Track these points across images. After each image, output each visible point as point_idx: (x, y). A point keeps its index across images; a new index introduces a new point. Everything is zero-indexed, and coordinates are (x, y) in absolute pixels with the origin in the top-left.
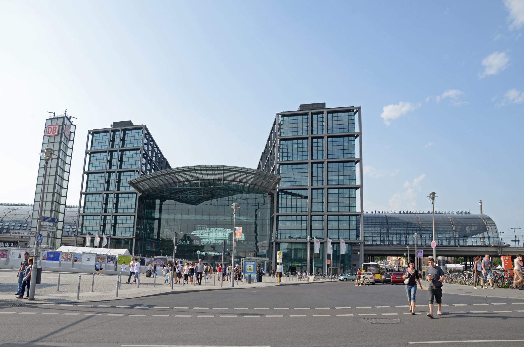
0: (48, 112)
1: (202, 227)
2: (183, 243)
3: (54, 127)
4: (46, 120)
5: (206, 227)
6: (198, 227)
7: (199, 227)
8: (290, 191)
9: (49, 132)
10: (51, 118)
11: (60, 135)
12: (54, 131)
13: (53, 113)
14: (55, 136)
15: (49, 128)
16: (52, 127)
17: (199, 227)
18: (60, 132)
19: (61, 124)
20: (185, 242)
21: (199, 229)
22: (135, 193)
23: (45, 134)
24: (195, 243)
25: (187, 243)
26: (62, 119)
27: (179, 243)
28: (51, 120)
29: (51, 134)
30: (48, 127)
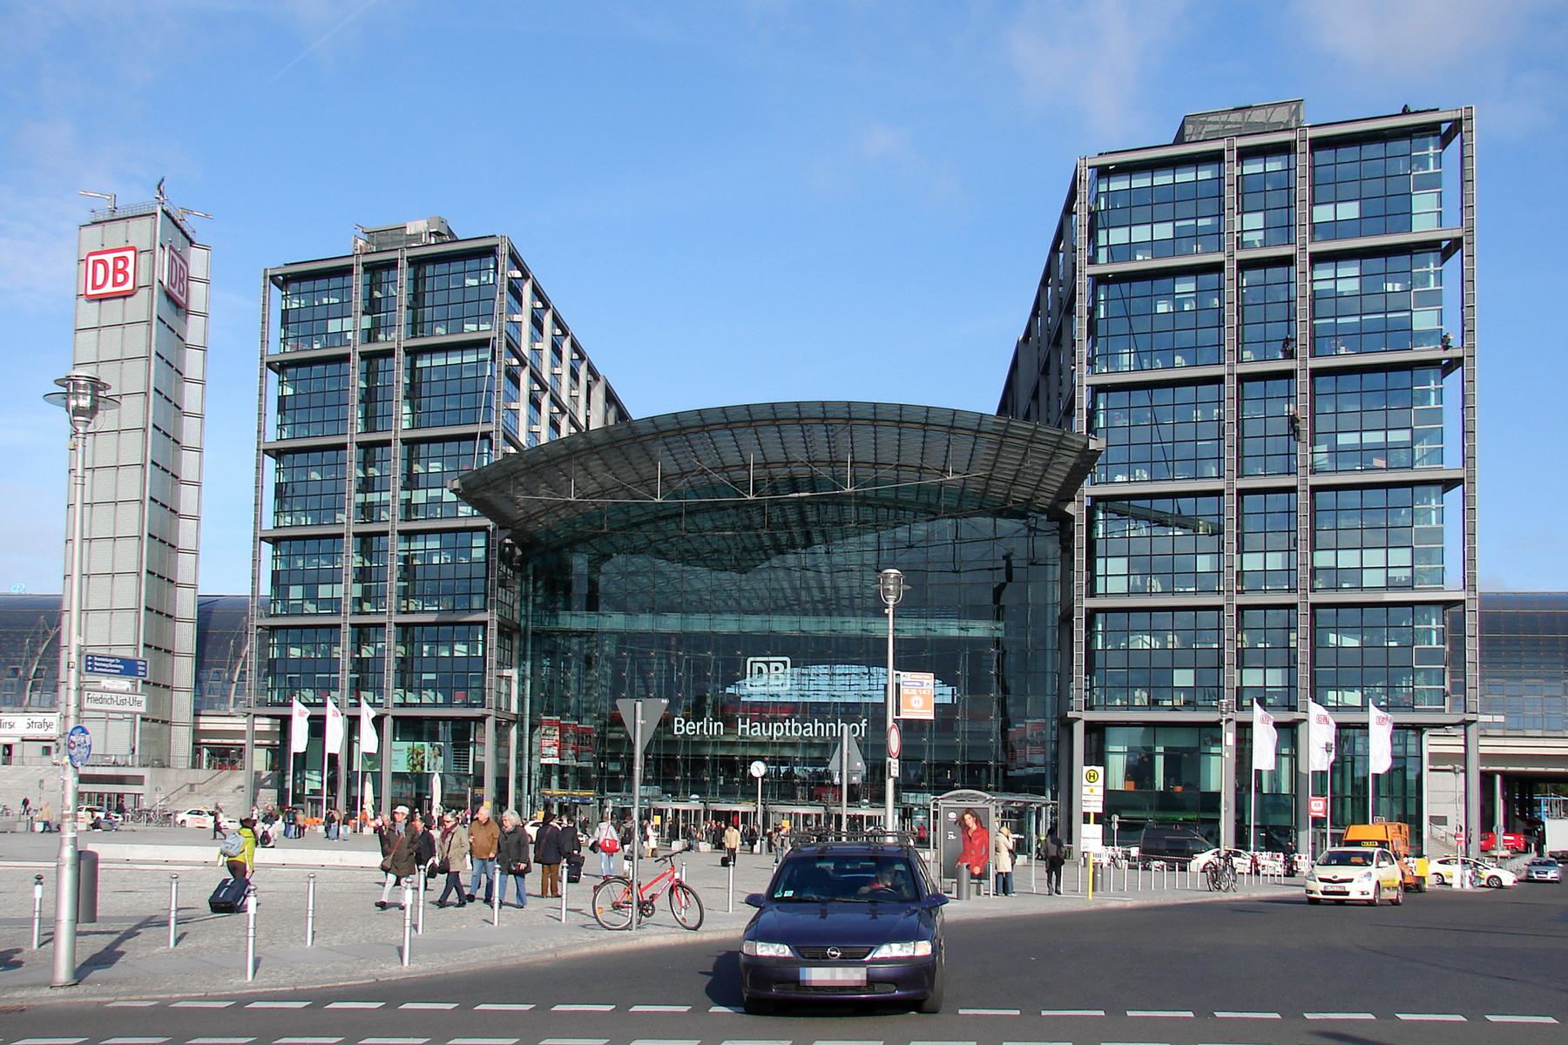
1: (768, 664)
2: (691, 731)
3: (116, 259)
5: (784, 663)
6: (752, 662)
7: (756, 666)
8: (1146, 503)
9: (99, 282)
10: (101, 218)
11: (144, 293)
12: (120, 278)
14: (125, 296)
16: (109, 258)
17: (756, 666)
20: (702, 727)
21: (755, 671)
22: (484, 529)
24: (744, 730)
25: (708, 731)
27: (676, 733)
28: (98, 228)
29: (109, 288)
30: (91, 259)
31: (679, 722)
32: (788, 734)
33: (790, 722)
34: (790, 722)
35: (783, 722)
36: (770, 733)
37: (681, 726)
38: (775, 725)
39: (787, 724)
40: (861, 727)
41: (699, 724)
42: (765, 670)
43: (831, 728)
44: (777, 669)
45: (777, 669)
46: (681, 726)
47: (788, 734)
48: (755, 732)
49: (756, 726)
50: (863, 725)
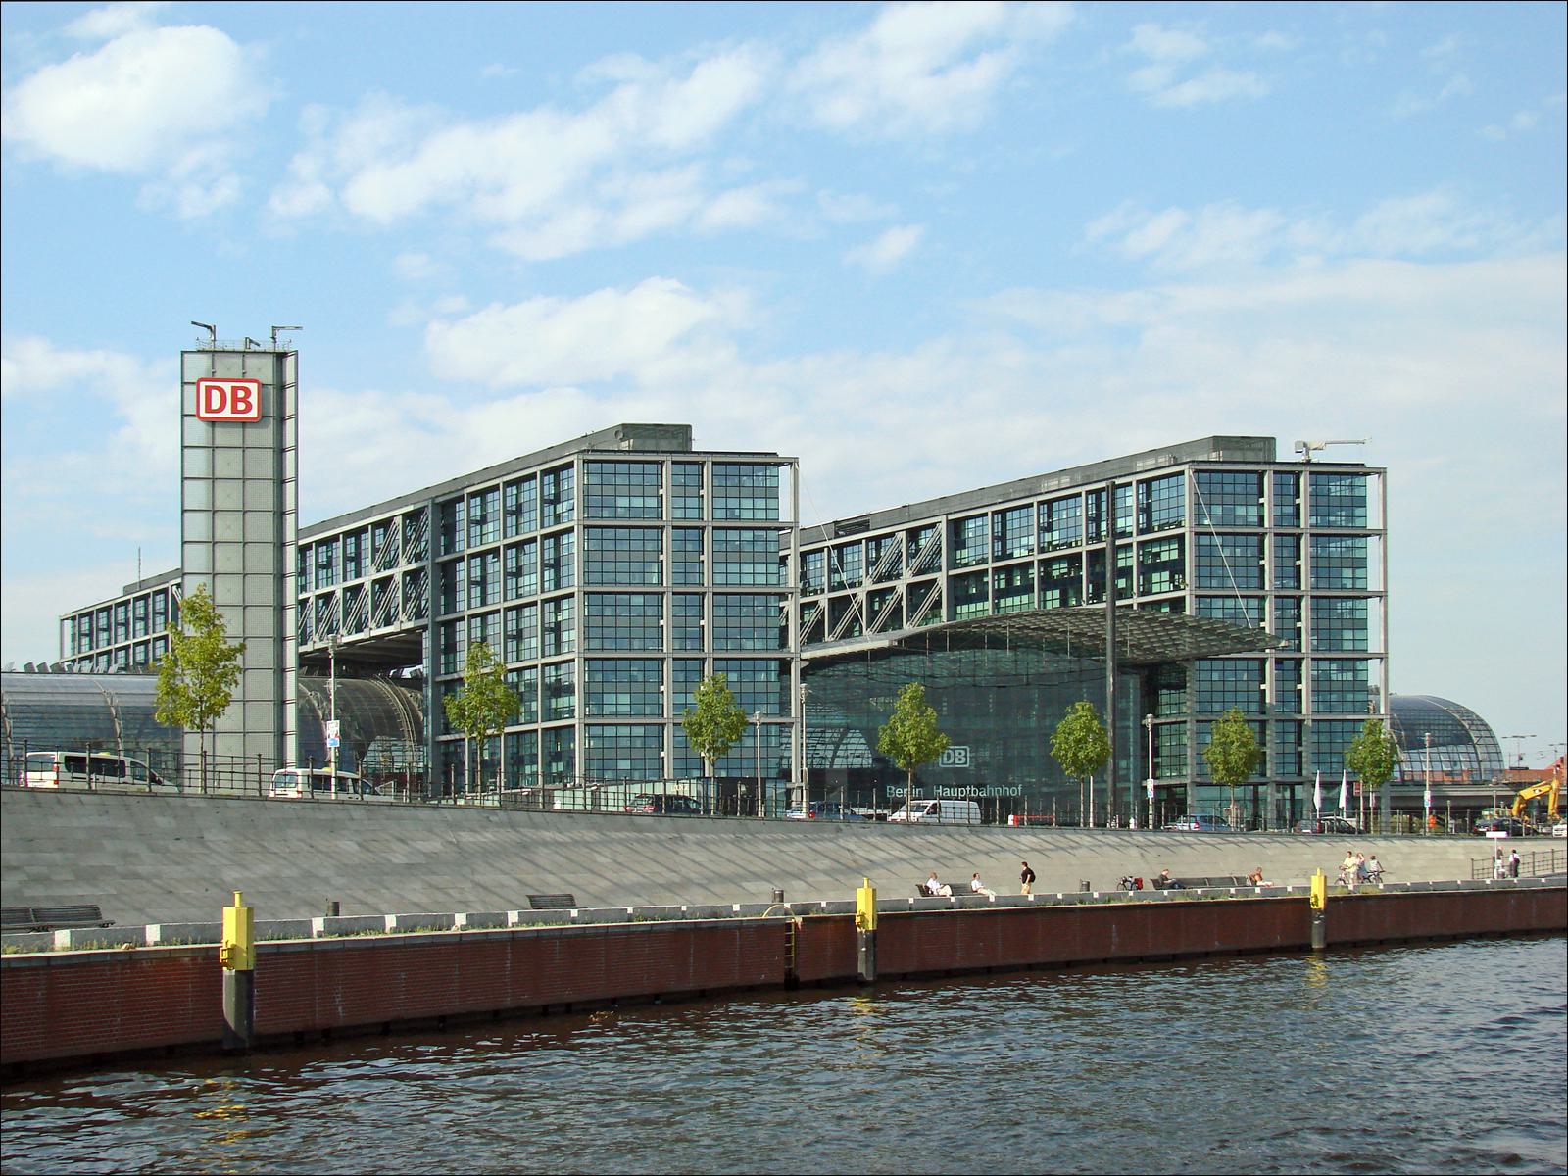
0: (194, 323)
1: (954, 750)
3: (235, 390)
4: (183, 353)
5: (966, 750)
9: (216, 403)
12: (241, 406)
13: (209, 328)
14: (244, 424)
15: (208, 390)
16: (227, 387)
18: (272, 410)
19: (267, 375)
23: (191, 409)
26: (269, 363)
29: (227, 413)
30: (203, 385)
31: (890, 789)
39: (968, 788)
41: (905, 790)
42: (952, 755)
44: (960, 753)
45: (960, 753)
46: (892, 791)
50: (1020, 788)
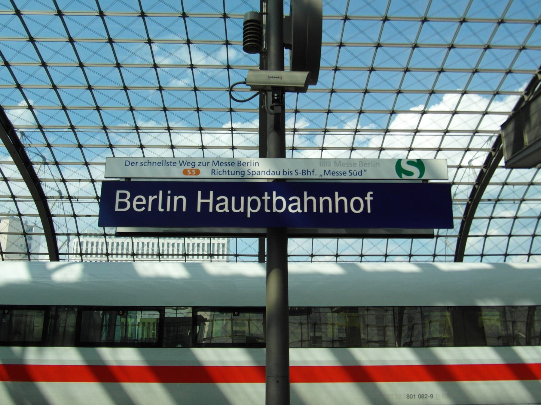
24: (205, 206)
32: (267, 210)
33: (270, 195)
34: (270, 195)
35: (261, 196)
36: (242, 209)
37: (126, 200)
38: (249, 199)
39: (266, 197)
40: (365, 202)
43: (326, 203)
46: (126, 200)
47: (267, 210)
48: (222, 207)
49: (223, 200)
50: (369, 198)
